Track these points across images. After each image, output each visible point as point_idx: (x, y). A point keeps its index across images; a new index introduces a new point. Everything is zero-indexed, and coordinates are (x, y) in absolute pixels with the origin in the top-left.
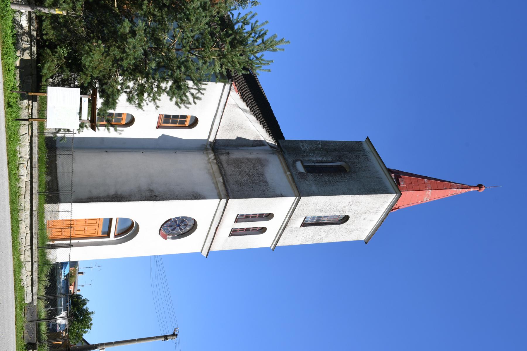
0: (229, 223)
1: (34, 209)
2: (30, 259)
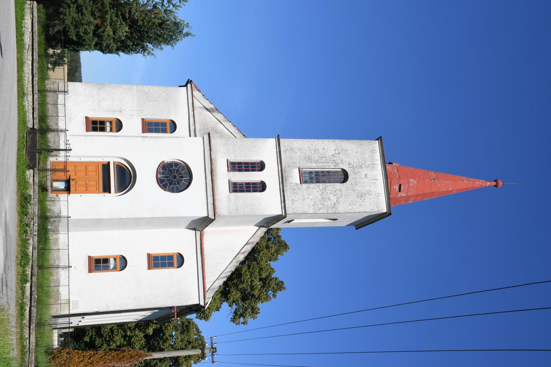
0: (224, 178)
1: (34, 58)
2: (31, 93)
